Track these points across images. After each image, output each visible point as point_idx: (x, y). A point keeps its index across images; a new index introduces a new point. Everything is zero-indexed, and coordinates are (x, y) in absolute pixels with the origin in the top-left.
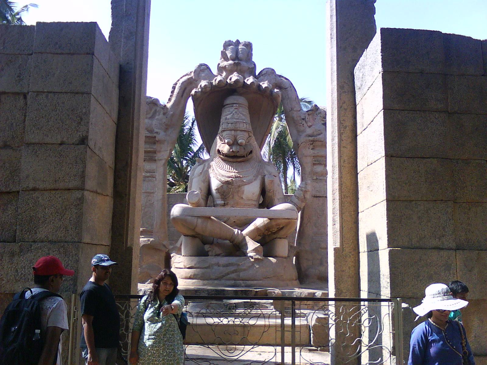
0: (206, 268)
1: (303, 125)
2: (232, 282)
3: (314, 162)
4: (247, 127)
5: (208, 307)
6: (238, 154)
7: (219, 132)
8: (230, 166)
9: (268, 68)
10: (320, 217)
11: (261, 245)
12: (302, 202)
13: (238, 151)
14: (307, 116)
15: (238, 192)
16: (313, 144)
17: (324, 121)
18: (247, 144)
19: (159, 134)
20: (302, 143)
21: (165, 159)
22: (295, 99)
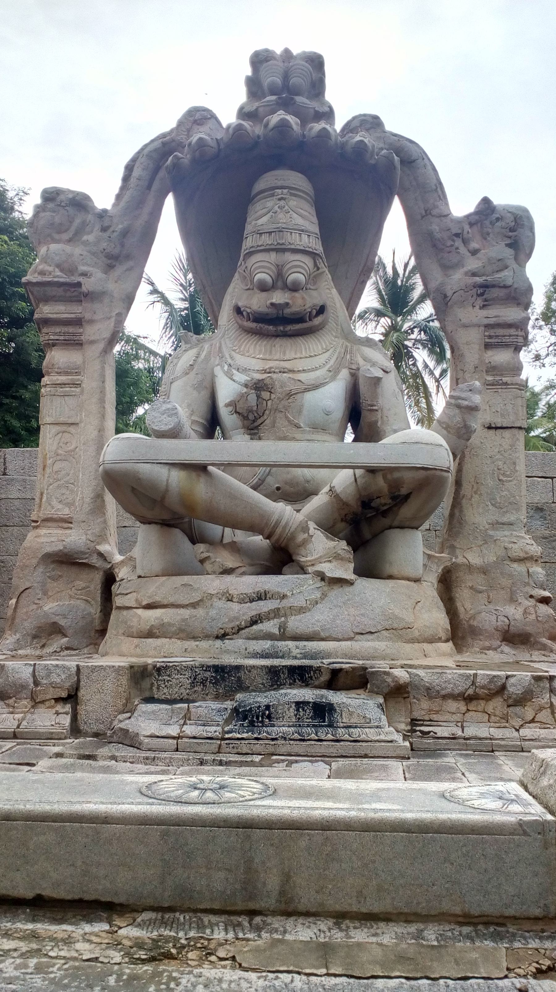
0: (194, 605)
1: (457, 248)
2: (266, 645)
3: (487, 340)
4: (309, 243)
5: (187, 717)
6: (287, 311)
7: (239, 264)
8: (265, 346)
9: (365, 115)
10: (505, 479)
11: (349, 544)
12: (459, 437)
13: (287, 304)
14: (467, 228)
15: (286, 408)
16: (482, 294)
17: (510, 237)
18: (312, 287)
19: (91, 275)
20: (454, 293)
21: (104, 339)
22: (434, 187)
